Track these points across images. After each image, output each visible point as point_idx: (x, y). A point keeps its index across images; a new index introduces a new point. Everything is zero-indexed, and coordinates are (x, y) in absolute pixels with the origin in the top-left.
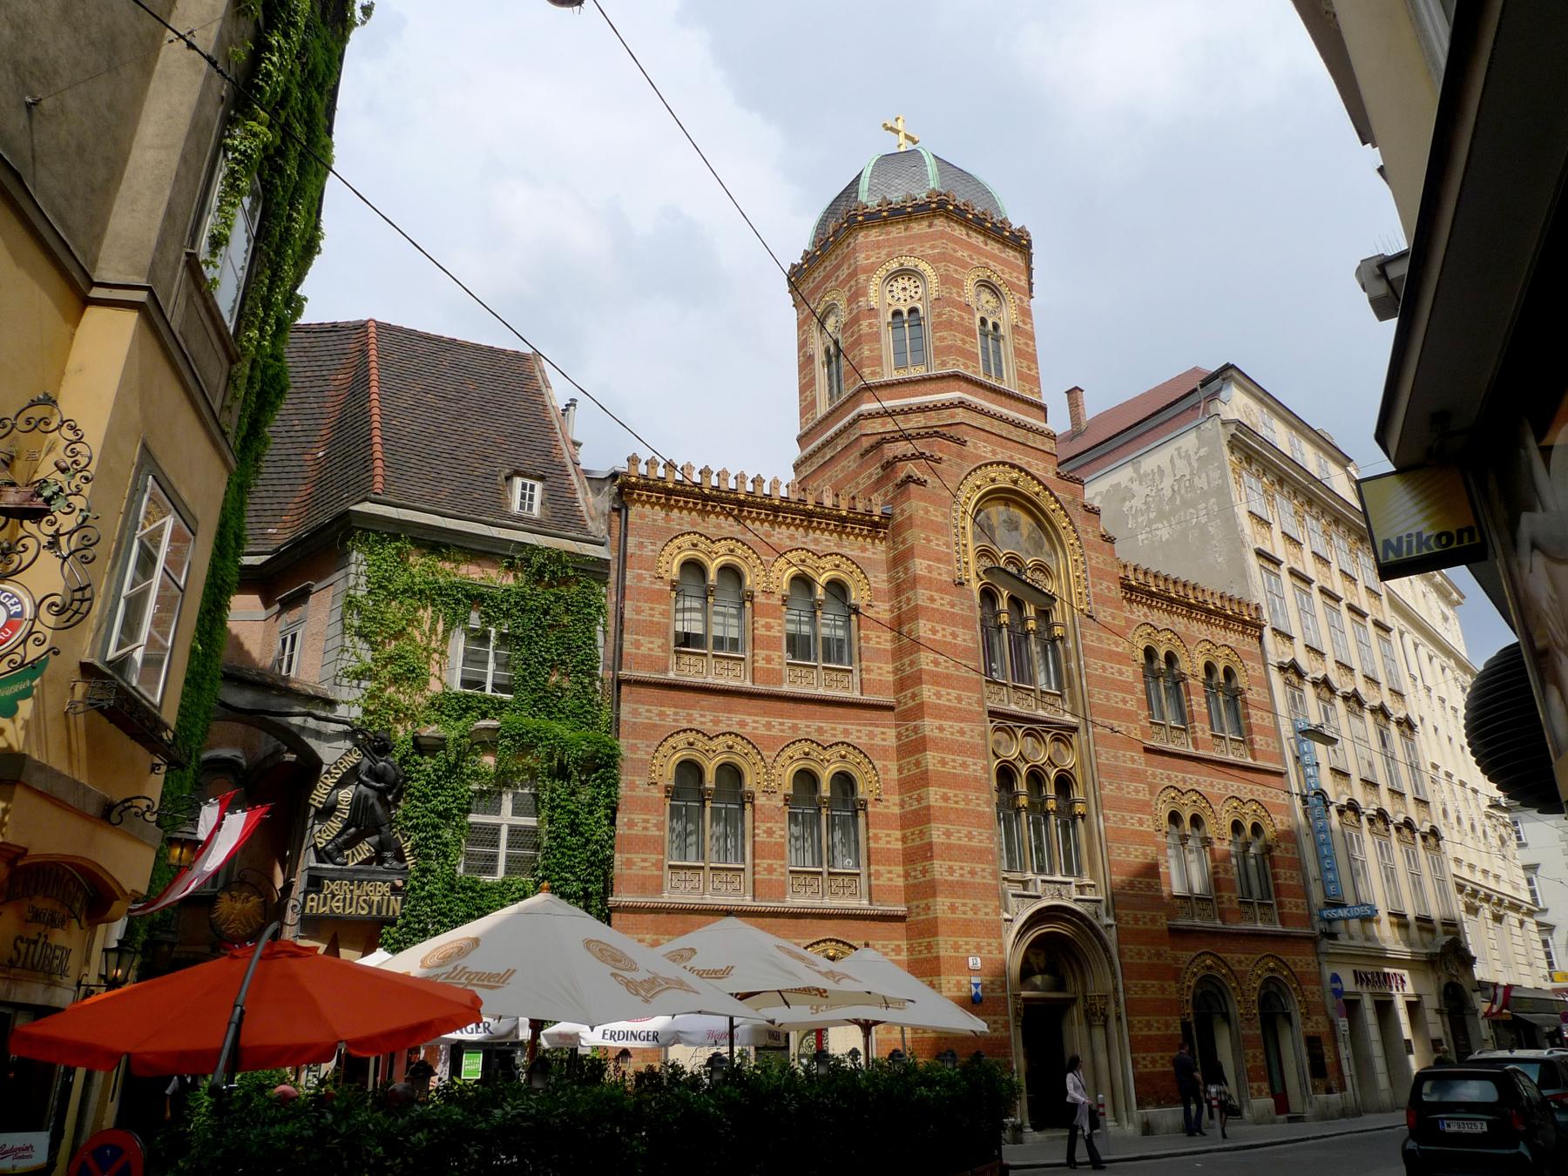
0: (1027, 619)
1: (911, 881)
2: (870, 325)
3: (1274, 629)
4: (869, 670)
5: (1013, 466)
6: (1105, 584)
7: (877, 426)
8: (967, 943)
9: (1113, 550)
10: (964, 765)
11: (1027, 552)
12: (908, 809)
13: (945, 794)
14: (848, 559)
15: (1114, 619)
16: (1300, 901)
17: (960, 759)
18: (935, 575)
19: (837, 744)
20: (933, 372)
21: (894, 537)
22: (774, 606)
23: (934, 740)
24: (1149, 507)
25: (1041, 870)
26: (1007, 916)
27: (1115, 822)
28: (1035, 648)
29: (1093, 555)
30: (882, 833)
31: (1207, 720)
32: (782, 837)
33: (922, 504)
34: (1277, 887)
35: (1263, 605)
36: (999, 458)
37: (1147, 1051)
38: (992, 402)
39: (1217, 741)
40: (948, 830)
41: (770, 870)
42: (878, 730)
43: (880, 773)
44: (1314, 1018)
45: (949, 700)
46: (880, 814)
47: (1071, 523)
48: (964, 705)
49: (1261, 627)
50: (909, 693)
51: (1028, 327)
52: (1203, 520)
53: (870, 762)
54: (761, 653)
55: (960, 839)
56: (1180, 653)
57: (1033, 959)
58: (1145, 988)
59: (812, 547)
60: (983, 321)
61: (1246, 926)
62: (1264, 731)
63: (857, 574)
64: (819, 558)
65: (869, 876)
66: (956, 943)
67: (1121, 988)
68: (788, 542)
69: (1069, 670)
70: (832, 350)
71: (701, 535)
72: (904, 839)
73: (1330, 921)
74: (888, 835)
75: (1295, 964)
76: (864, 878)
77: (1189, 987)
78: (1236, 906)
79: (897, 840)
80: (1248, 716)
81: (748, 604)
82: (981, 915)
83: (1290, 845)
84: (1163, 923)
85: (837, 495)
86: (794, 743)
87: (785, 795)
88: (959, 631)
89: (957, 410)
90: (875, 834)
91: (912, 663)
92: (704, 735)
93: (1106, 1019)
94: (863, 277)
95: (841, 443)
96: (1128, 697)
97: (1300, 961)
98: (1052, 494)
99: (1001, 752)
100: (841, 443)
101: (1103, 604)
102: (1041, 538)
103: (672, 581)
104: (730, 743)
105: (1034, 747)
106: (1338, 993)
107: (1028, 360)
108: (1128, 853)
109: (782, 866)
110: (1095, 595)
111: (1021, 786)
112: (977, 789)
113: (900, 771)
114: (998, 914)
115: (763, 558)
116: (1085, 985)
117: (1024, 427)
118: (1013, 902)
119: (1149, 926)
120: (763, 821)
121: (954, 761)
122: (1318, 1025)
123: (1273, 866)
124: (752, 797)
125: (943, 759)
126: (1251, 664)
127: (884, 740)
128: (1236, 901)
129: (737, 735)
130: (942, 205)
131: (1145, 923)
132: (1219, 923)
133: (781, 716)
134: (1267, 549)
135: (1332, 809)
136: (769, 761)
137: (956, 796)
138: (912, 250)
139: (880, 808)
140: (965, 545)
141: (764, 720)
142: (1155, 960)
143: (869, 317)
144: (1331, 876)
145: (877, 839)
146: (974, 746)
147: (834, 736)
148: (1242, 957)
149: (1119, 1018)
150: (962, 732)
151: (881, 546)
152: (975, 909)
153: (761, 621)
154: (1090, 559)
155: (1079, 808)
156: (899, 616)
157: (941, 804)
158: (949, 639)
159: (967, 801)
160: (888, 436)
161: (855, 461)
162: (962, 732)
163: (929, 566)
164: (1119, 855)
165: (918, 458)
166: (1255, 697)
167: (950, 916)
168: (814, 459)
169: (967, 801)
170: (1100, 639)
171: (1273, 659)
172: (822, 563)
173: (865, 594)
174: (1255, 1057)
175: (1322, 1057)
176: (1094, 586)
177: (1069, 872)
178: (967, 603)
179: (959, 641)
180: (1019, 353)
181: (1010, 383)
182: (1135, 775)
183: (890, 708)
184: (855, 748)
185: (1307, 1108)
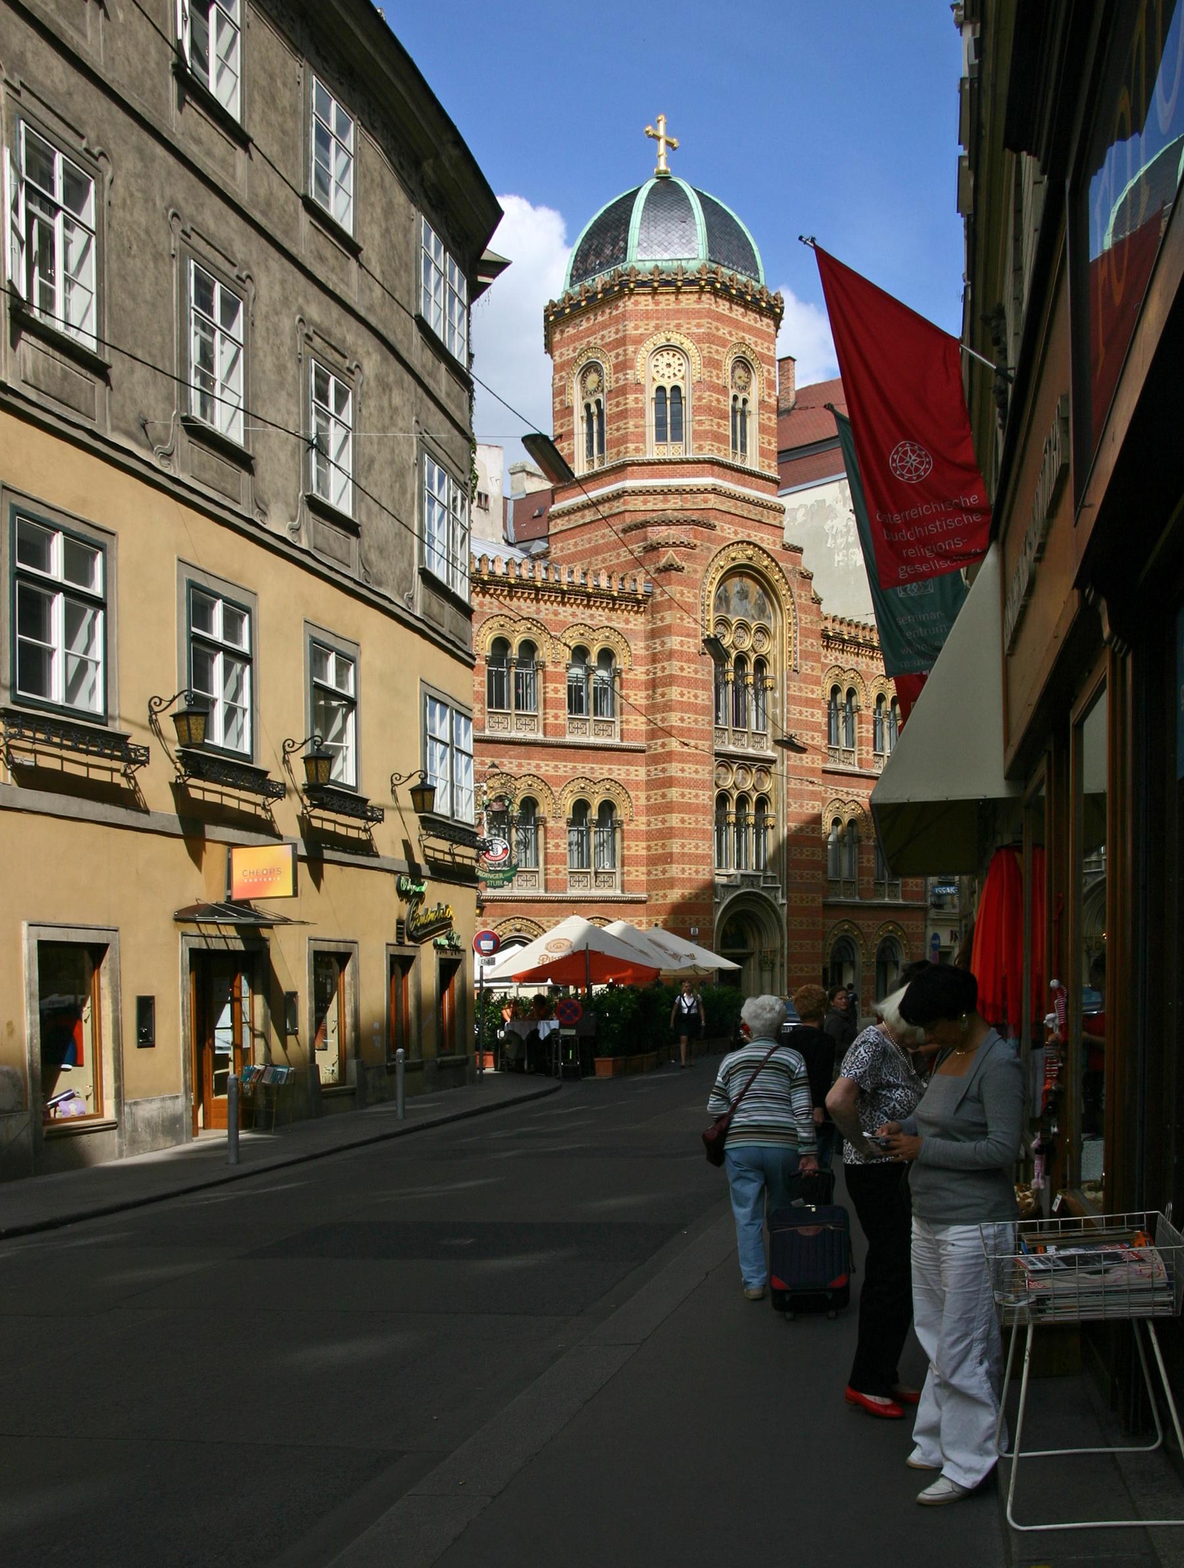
1: (652, 877)
2: (636, 400)
4: (628, 722)
6: (810, 641)
9: (819, 609)
10: (697, 796)
11: (753, 617)
12: (653, 827)
17: (694, 792)
18: (685, 648)
20: (690, 456)
21: (653, 613)
23: (677, 779)
24: (848, 532)
29: (803, 616)
30: (632, 844)
31: (872, 743)
32: (565, 849)
36: (739, 538)
38: (738, 483)
39: (877, 759)
41: (557, 872)
42: (632, 769)
43: (633, 800)
47: (789, 589)
50: (659, 742)
54: (551, 712)
56: (859, 689)
59: (588, 622)
60: (735, 398)
63: (622, 645)
64: (594, 631)
65: (623, 874)
68: (571, 619)
69: (774, 715)
72: (649, 848)
74: (637, 846)
76: (618, 875)
85: (610, 577)
88: (700, 692)
89: (711, 496)
90: (628, 845)
91: (663, 720)
94: (631, 349)
96: (816, 734)
98: (777, 565)
99: (720, 783)
102: (764, 604)
104: (530, 782)
108: (801, 853)
109: (565, 869)
111: (732, 807)
112: (704, 813)
113: (648, 798)
116: (761, 944)
117: (762, 506)
121: (690, 793)
124: (544, 821)
127: (637, 776)
129: (534, 776)
130: (711, 283)
133: (565, 761)
138: (678, 326)
139: (632, 826)
140: (709, 621)
141: (552, 764)
143: (636, 392)
145: (629, 848)
146: (704, 782)
147: (602, 774)
150: (696, 772)
151: (641, 619)
153: (551, 686)
154: (801, 620)
155: (770, 822)
156: (654, 680)
158: (692, 700)
159: (697, 822)
160: (649, 516)
162: (696, 772)
163: (682, 641)
170: (800, 689)
172: (595, 635)
173: (627, 660)
179: (699, 701)
184: (616, 782)
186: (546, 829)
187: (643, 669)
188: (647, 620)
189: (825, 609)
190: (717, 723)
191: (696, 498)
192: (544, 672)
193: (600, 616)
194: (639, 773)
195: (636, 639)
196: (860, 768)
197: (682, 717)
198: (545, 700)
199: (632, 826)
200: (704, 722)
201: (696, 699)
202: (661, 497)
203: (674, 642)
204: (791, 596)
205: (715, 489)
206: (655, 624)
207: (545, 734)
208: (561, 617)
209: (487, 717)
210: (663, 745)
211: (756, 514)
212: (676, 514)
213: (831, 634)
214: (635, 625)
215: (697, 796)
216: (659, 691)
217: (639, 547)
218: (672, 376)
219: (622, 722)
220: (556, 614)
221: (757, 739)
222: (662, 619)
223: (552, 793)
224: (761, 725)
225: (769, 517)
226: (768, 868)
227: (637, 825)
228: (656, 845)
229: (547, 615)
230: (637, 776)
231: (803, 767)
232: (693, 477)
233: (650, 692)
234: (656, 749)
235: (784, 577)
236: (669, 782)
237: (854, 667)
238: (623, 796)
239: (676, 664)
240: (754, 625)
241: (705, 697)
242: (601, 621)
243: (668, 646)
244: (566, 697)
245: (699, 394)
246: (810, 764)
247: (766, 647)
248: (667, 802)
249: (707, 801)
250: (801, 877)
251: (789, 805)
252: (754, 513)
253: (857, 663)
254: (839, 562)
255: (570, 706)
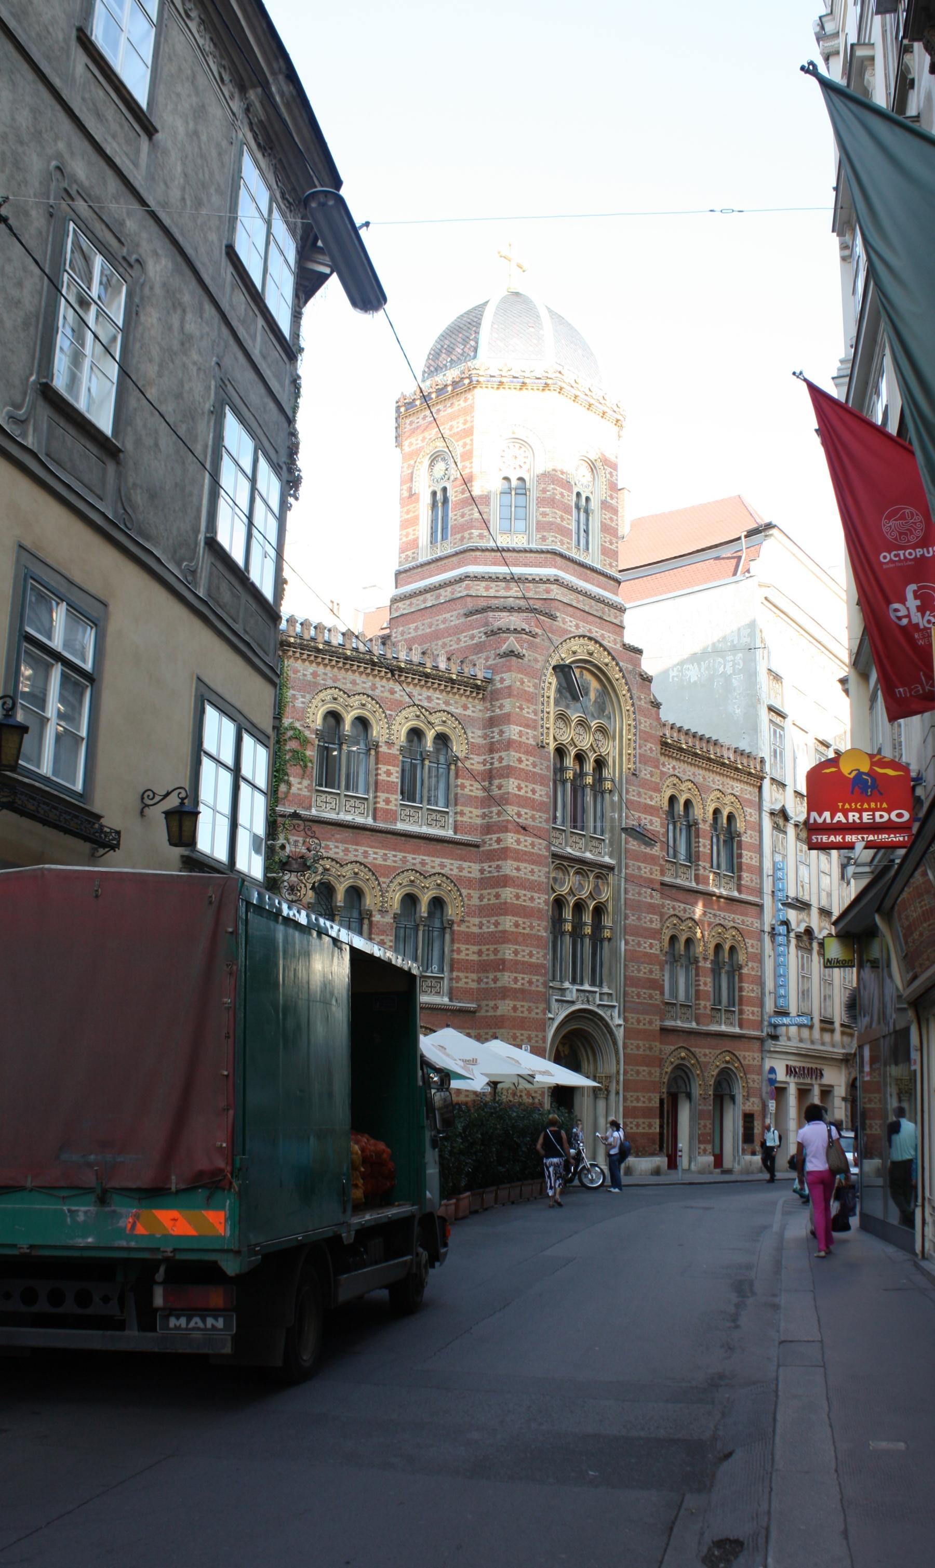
0: (586, 774)
1: (483, 985)
3: (772, 779)
4: (462, 814)
5: (590, 639)
6: (649, 745)
7: (480, 589)
8: (522, 1035)
9: (658, 715)
11: (593, 715)
12: (485, 929)
13: (517, 921)
14: (452, 716)
15: (652, 776)
16: (756, 1009)
17: (529, 894)
18: (524, 739)
19: (434, 874)
20: (533, 546)
21: (492, 700)
22: (395, 756)
25: (574, 982)
26: (550, 1016)
27: (633, 946)
28: (589, 798)
29: (643, 719)
30: (463, 947)
31: (709, 859)
33: (520, 676)
34: (741, 997)
35: (767, 759)
37: (635, 1118)
38: (580, 577)
40: (516, 949)
42: (465, 865)
43: (466, 899)
44: (752, 1100)
45: (526, 846)
46: (463, 932)
48: (536, 850)
49: (762, 778)
50: (495, 837)
51: (613, 502)
52: (729, 671)
53: (458, 890)
54: (382, 796)
55: (524, 956)
57: (561, 1048)
58: (638, 1073)
59: (425, 704)
60: (578, 494)
61: (714, 1028)
62: (751, 869)
65: (451, 979)
66: (515, 1034)
67: (622, 1071)
69: (612, 819)
70: (439, 496)
71: (340, 690)
73: (775, 1026)
74: (467, 949)
75: (745, 1058)
77: (666, 1072)
78: (708, 1012)
79: (474, 953)
80: (740, 856)
81: (373, 752)
82: (533, 1015)
83: (755, 965)
84: (657, 1024)
85: (449, 659)
86: (403, 872)
87: (395, 914)
88: (538, 788)
89: (553, 587)
91: (499, 814)
92: (337, 862)
93: (608, 1092)
95: (446, 594)
97: (749, 1056)
98: (617, 664)
99: (556, 887)
100: (446, 594)
101: (645, 764)
102: (604, 703)
103: (317, 730)
104: (356, 870)
105: (580, 883)
106: (772, 1082)
107: (610, 534)
108: (639, 971)
110: (640, 754)
112: (539, 918)
113: (481, 898)
114: (545, 1014)
115: (388, 712)
117: (603, 602)
118: (554, 1005)
119: (647, 1027)
120: (378, 934)
122: (753, 1105)
123: (741, 980)
125: (517, 894)
126: (749, 810)
127: (470, 872)
128: (709, 1008)
129: (361, 864)
131: (644, 1024)
132: (694, 1025)
133: (395, 850)
134: (777, 705)
135: (792, 935)
136: (384, 886)
137: (524, 923)
141: (381, 852)
142: (648, 1052)
144: (782, 992)
145: (459, 951)
146: (540, 884)
148: (707, 1051)
149: (617, 1093)
150: (532, 872)
151: (480, 706)
152: (530, 1010)
153: (383, 768)
154: (640, 723)
155: (607, 933)
156: (490, 770)
157: (513, 929)
158: (530, 795)
159: (531, 927)
161: (458, 618)
163: (520, 731)
164: (633, 971)
165: (519, 633)
166: (749, 840)
167: (513, 1014)
168: (414, 600)
169: (531, 927)
170: (639, 794)
171: (767, 806)
174: (705, 1126)
175: (752, 1129)
176: (640, 747)
177: (593, 984)
178: (545, 764)
179: (537, 797)
180: (605, 528)
181: (594, 559)
182: (652, 909)
183: (477, 846)
184: (448, 878)
185: (736, 1165)
186: (371, 923)
187: (481, 759)
188: (486, 708)
189: (666, 715)
190: (555, 823)
191: (539, 587)
192: (377, 753)
193: (438, 699)
194: (472, 869)
195: (474, 727)
196: (697, 883)
197: (519, 812)
198: (376, 783)
199: (463, 928)
200: (539, 820)
201: (534, 794)
202: (503, 584)
203: (513, 731)
204: (631, 698)
205: (557, 580)
206: (493, 711)
207: (375, 819)
208: (397, 696)
209: (314, 796)
210: (499, 841)
211: (597, 610)
212: (518, 601)
213: (669, 741)
214: (473, 712)
215: (532, 899)
216: (496, 782)
217: (480, 632)
218: (518, 468)
219: (456, 813)
220: (392, 692)
221: (595, 843)
222: (501, 707)
223: (379, 884)
224: (599, 830)
225: (610, 615)
226: (605, 984)
227: (468, 927)
228: (488, 950)
229: (382, 692)
230: (470, 872)
231: (641, 877)
232: (536, 567)
233: (486, 784)
234: (490, 845)
235: (624, 677)
236: (504, 881)
237: (691, 778)
238: (455, 894)
239: (515, 755)
240: (594, 724)
241: (541, 793)
242: (438, 704)
243: (506, 735)
244: (399, 781)
245: (543, 486)
246: (648, 875)
247: (609, 749)
248: (501, 903)
249: (542, 906)
250: (639, 996)
251: (626, 917)
252: (596, 608)
253: (694, 774)
254: (673, 677)
255: (402, 793)
